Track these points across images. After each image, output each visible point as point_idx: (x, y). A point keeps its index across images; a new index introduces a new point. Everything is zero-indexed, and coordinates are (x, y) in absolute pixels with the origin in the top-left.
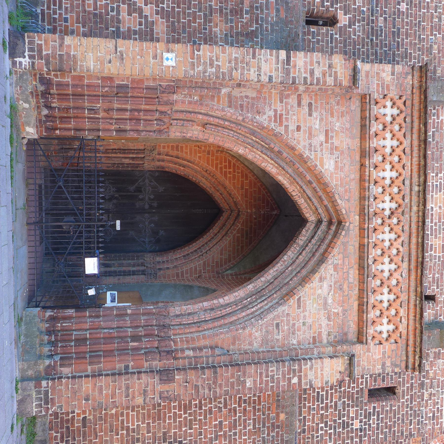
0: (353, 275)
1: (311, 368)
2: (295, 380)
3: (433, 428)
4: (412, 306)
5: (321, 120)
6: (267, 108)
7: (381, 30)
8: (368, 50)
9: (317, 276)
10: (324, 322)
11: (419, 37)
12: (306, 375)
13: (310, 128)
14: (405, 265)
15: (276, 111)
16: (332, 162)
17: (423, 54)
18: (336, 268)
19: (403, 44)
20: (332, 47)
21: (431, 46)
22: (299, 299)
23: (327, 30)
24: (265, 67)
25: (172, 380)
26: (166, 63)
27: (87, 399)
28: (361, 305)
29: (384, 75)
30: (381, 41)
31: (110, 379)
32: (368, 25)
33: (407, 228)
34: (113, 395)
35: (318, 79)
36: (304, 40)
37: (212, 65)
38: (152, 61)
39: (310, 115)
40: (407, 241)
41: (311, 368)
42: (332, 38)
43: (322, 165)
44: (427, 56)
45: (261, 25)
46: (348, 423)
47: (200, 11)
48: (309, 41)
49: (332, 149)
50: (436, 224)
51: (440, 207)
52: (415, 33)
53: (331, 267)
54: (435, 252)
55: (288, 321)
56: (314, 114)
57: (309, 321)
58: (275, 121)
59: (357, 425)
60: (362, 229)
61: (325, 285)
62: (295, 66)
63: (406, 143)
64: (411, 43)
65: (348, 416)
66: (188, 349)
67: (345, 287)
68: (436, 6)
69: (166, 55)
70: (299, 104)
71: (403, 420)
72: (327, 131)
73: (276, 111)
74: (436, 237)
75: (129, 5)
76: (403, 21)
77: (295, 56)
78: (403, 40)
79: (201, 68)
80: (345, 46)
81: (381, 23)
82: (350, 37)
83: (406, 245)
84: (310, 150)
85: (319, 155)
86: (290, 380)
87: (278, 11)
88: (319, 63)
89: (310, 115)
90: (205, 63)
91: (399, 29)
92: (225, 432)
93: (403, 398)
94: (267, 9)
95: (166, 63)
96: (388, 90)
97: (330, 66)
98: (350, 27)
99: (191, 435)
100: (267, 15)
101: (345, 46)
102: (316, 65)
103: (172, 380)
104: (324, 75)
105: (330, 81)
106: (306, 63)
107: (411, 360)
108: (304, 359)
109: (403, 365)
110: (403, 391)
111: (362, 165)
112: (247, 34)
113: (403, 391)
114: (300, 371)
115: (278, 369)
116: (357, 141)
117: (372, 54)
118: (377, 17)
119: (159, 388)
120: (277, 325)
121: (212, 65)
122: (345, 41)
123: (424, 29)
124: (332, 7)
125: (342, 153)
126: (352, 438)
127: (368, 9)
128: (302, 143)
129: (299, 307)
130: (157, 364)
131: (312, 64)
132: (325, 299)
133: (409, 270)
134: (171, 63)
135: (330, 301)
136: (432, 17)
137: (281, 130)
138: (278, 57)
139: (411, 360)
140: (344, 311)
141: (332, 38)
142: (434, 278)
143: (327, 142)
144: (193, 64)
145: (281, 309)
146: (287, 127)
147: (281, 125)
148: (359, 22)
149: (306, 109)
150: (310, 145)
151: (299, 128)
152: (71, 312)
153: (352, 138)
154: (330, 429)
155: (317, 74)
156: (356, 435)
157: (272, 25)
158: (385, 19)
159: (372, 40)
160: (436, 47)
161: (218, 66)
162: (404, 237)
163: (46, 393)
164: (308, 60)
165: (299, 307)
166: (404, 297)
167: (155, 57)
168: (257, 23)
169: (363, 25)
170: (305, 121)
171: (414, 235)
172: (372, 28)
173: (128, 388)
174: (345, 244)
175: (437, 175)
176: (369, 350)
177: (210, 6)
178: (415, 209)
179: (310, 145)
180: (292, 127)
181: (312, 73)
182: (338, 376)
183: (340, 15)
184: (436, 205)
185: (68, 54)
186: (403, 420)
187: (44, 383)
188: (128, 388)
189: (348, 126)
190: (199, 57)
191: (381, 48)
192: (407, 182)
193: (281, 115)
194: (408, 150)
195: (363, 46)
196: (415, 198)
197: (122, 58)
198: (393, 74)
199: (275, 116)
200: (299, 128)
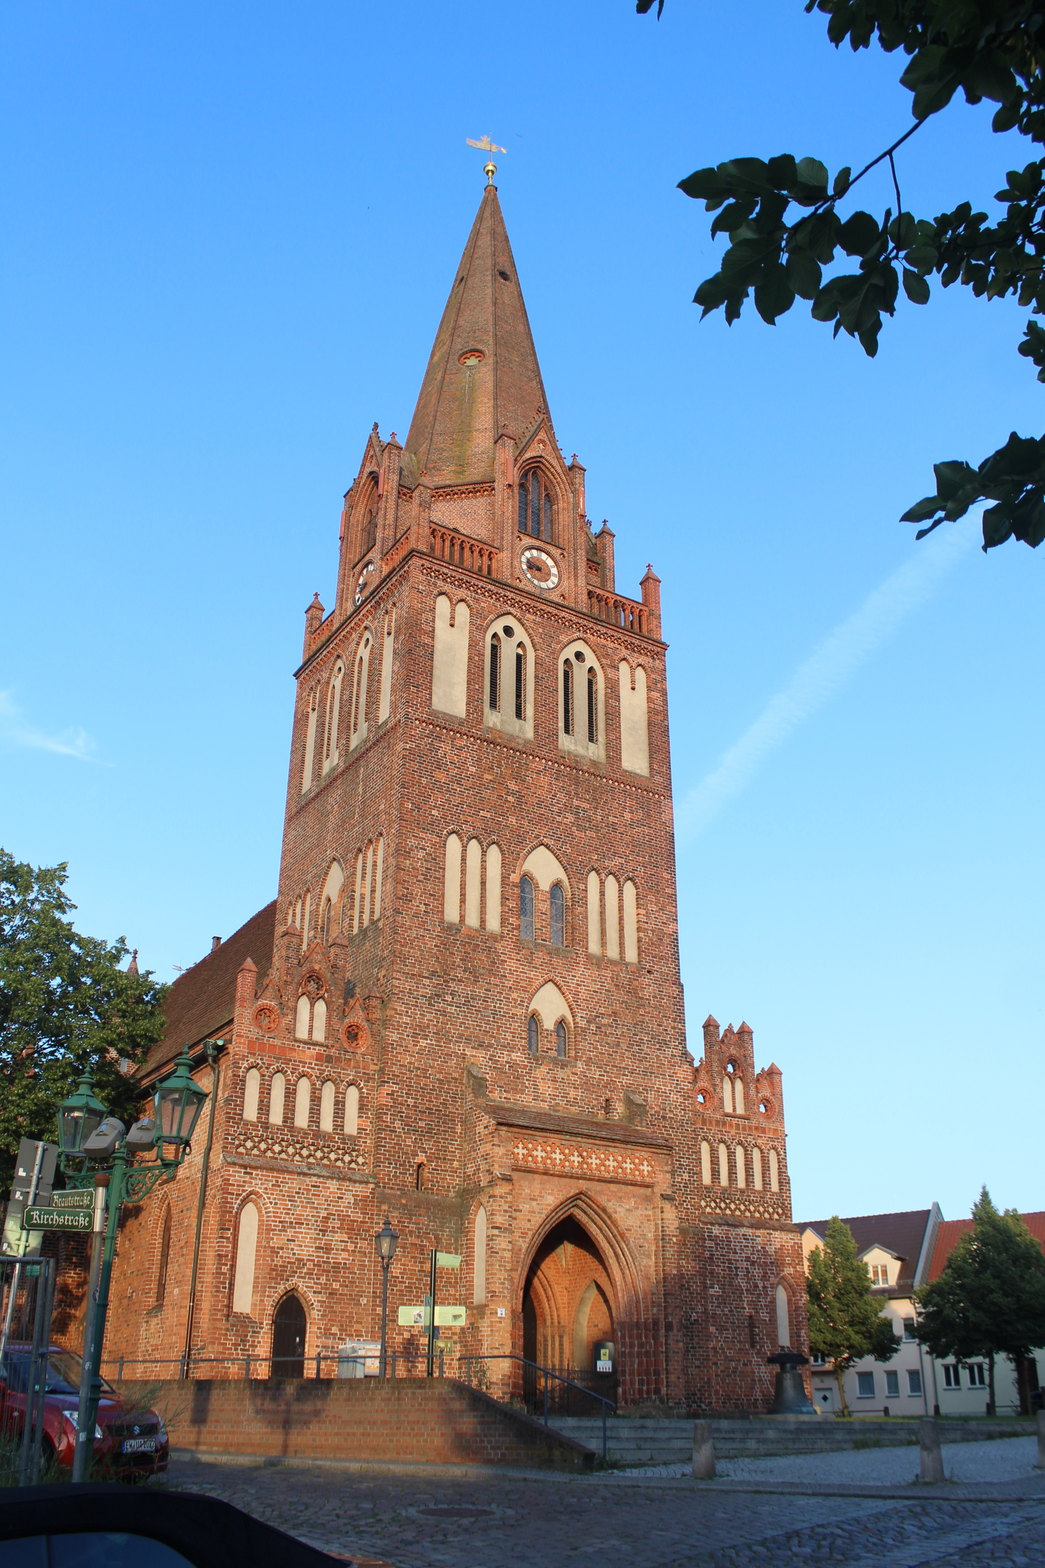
0: (613, 1187)
1: (668, 1227)
2: (674, 1239)
3: (691, 1111)
4: (635, 1148)
5: (524, 1203)
6: (518, 1243)
7: (429, 1124)
8: (442, 1139)
9: (614, 1215)
10: (639, 1212)
11: (431, 1089)
12: (672, 1231)
13: (529, 1212)
14: (611, 1149)
15: (519, 1237)
16: (549, 1197)
17: (443, 1088)
18: (609, 1201)
19: (438, 1106)
20: (442, 1170)
21: (438, 1080)
22: (626, 1230)
23: (429, 1173)
24: (503, 1246)
25: (671, 1323)
26: (504, 1315)
27: (679, 1378)
28: (631, 1185)
29: (500, 1153)
30: (436, 1126)
31: (670, 1363)
32: (424, 1136)
33: (590, 1146)
34: (678, 1361)
35: (510, 1207)
36: (437, 1194)
37: (504, 1284)
38: (503, 1324)
39: (521, 1211)
40: (597, 1147)
41: (668, 1227)
42: (435, 1170)
43: (549, 1205)
44: (445, 1084)
45: (431, 1230)
46: (685, 1183)
47: (422, 1280)
48: (437, 1189)
49: (541, 1196)
50: (560, 1093)
51: (549, 1087)
52: (428, 1093)
53: (610, 1204)
54: (578, 1095)
55: (639, 1239)
56: (521, 1208)
57: (639, 1223)
58: (525, 1237)
59: (686, 1176)
60: (590, 1180)
61: (619, 1209)
62: (502, 1224)
63: (540, 1140)
64: (436, 1098)
65: (681, 1183)
66: (652, 1311)
67: (620, 1194)
68: (409, 1071)
69: (499, 1315)
70: (515, 1219)
71: (685, 1137)
72: (531, 1199)
73: (519, 1237)
74: (568, 1094)
75: (420, 1336)
76: (420, 1103)
77: (496, 1223)
78: (434, 1105)
79: (506, 1291)
80: (440, 1158)
81: (422, 1124)
82: (434, 1154)
83: (601, 1147)
84: (542, 1213)
85: (544, 1206)
86: (674, 1243)
87: (420, 1215)
88: (500, 1206)
89: (521, 1211)
90: (503, 1288)
91: (427, 1108)
92: (686, 1282)
93: (671, 1135)
94: (419, 1224)
95: (504, 1315)
96: (507, 1151)
97: (501, 1197)
98: (426, 1152)
99: (686, 1308)
100: (423, 1224)
101: (440, 1158)
102: (501, 1208)
103: (671, 1323)
104: (506, 1202)
105: (510, 1198)
106: (500, 1215)
107: (665, 1152)
108: (662, 1231)
109: (667, 1157)
110: (667, 1134)
111: (552, 1175)
112: (437, 1243)
113: (667, 1134)
114: (669, 1235)
115: (668, 1251)
116: (536, 1176)
117: (445, 1135)
118: (420, 1127)
119: (675, 1331)
120: (640, 1247)
121: (504, 1284)
122: (436, 1158)
123: (425, 1085)
124: (413, 1166)
125: (543, 1189)
126: (694, 1181)
127: (414, 1134)
128: (538, 1219)
129: (630, 1230)
130: (663, 1331)
131: (500, 1211)
132: (627, 1210)
133: (615, 1147)
134: (504, 1313)
135: (628, 1207)
136: (417, 1076)
137: (530, 1233)
138: (497, 1236)
139: (665, 1152)
140: (634, 1196)
141: (435, 1170)
142: (596, 1099)
143: (536, 1200)
144: (504, 1297)
145: (632, 1244)
146: (528, 1229)
147: (527, 1234)
148: (422, 1144)
149: (518, 1213)
150: (539, 1213)
151: (529, 1221)
152: (620, 1390)
153: (534, 1179)
154: (687, 1198)
155: (506, 1208)
156: (693, 1177)
157: (430, 1221)
158: (420, 1119)
159: (435, 1134)
160: (438, 1075)
161: (504, 1279)
162: (595, 1148)
163: (675, 1403)
164: (498, 1213)
165: (630, 1230)
166: (629, 1152)
167: (501, 1322)
168: (429, 1234)
169: (425, 1140)
170: (525, 1215)
171: (595, 1141)
172: (427, 1132)
173: (674, 1352)
174: (596, 1191)
175: (527, 1087)
176: (658, 1182)
177: (419, 1271)
178: (579, 1139)
179: (539, 1213)
180: (528, 1225)
181: (505, 1211)
182: (674, 1208)
183: (418, 1160)
184: (547, 1091)
185: (502, 1380)
186: (685, 1137)
187: (670, 1404)
188: (674, 1352)
189: (527, 1183)
190: (499, 1292)
191: (440, 1126)
192: (563, 1142)
193: (522, 1233)
194: (545, 1140)
195: (440, 1142)
196: (573, 1138)
197: (502, 1345)
198: (499, 1146)
199: (522, 1237)
200: (529, 1221)
